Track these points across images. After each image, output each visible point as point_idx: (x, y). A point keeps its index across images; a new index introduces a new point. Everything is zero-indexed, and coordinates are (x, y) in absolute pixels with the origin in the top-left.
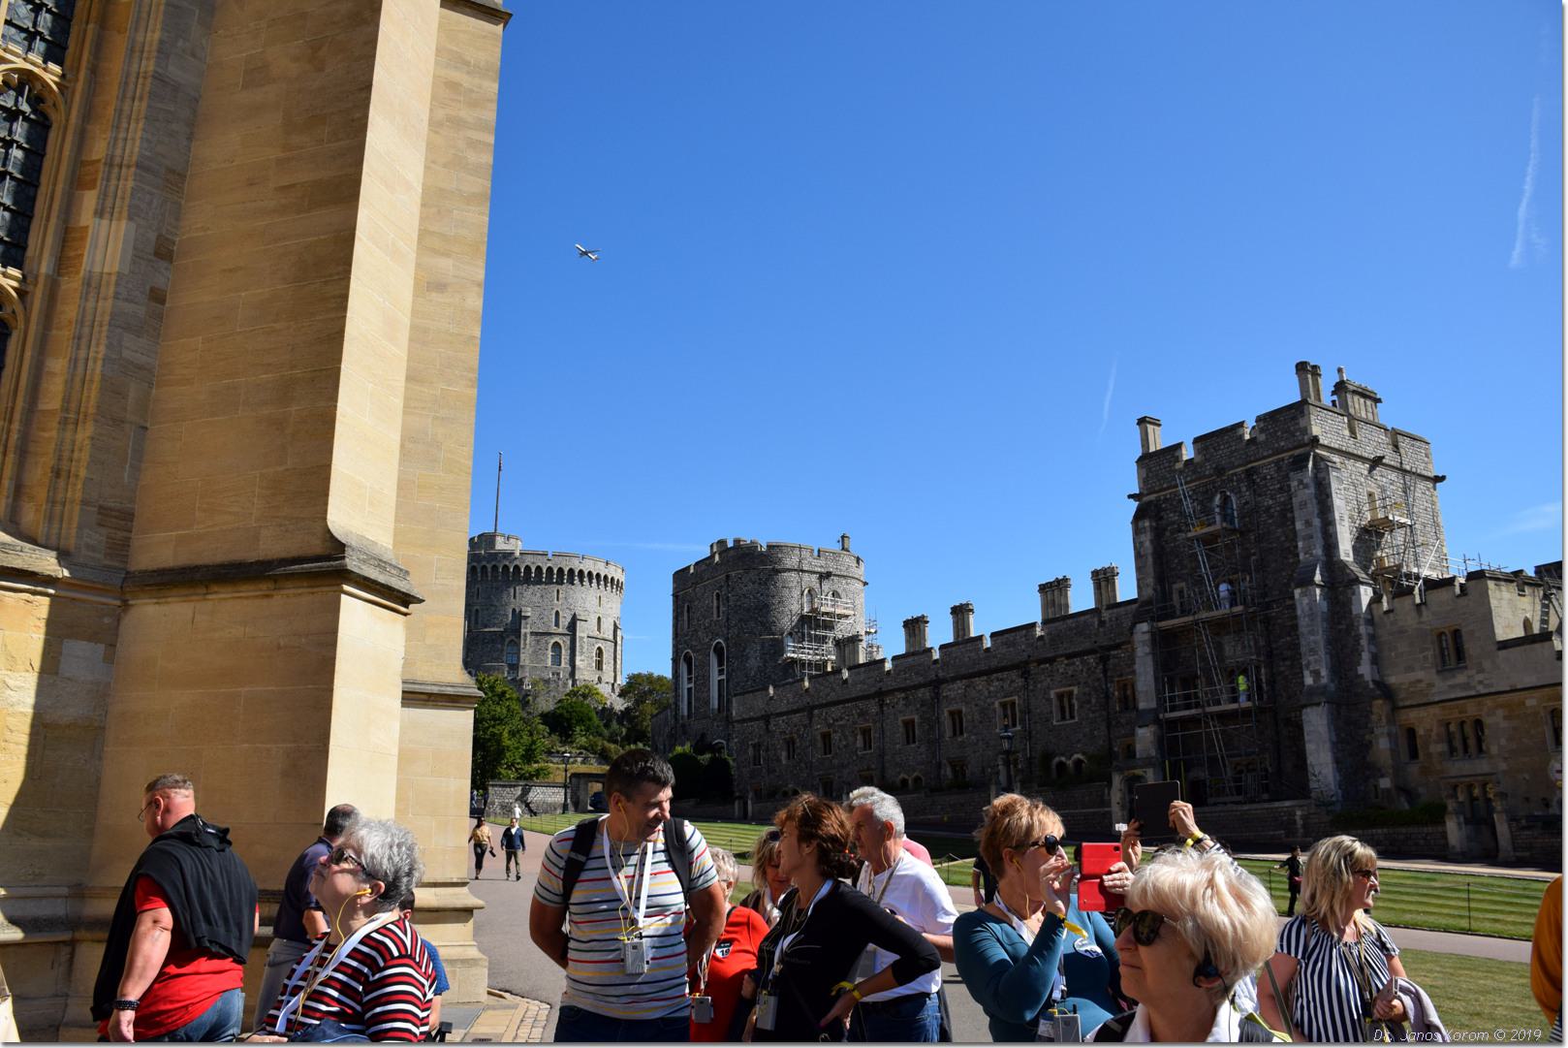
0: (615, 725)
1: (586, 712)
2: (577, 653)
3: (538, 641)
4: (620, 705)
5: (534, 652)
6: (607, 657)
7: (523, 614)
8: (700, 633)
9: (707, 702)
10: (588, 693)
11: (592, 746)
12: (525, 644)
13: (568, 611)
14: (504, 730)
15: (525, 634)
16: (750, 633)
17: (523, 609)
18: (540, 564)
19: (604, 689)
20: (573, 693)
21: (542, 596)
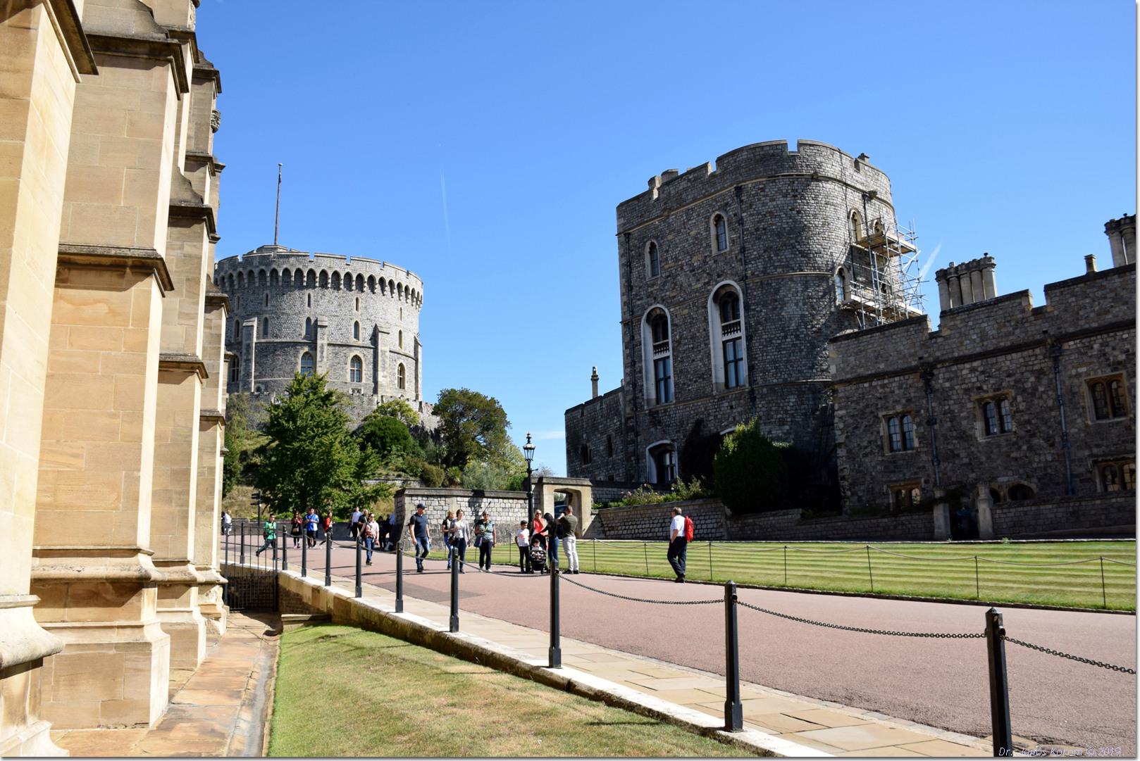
0: (431, 444)
1: (401, 428)
2: (380, 369)
4: (432, 422)
5: (332, 366)
6: (409, 374)
7: (319, 323)
8: (681, 279)
9: (706, 374)
10: (393, 410)
11: (409, 465)
12: (322, 357)
13: (368, 322)
14: (335, 439)
17: (320, 318)
18: (338, 270)
19: (414, 406)
20: (382, 410)
21: (340, 305)
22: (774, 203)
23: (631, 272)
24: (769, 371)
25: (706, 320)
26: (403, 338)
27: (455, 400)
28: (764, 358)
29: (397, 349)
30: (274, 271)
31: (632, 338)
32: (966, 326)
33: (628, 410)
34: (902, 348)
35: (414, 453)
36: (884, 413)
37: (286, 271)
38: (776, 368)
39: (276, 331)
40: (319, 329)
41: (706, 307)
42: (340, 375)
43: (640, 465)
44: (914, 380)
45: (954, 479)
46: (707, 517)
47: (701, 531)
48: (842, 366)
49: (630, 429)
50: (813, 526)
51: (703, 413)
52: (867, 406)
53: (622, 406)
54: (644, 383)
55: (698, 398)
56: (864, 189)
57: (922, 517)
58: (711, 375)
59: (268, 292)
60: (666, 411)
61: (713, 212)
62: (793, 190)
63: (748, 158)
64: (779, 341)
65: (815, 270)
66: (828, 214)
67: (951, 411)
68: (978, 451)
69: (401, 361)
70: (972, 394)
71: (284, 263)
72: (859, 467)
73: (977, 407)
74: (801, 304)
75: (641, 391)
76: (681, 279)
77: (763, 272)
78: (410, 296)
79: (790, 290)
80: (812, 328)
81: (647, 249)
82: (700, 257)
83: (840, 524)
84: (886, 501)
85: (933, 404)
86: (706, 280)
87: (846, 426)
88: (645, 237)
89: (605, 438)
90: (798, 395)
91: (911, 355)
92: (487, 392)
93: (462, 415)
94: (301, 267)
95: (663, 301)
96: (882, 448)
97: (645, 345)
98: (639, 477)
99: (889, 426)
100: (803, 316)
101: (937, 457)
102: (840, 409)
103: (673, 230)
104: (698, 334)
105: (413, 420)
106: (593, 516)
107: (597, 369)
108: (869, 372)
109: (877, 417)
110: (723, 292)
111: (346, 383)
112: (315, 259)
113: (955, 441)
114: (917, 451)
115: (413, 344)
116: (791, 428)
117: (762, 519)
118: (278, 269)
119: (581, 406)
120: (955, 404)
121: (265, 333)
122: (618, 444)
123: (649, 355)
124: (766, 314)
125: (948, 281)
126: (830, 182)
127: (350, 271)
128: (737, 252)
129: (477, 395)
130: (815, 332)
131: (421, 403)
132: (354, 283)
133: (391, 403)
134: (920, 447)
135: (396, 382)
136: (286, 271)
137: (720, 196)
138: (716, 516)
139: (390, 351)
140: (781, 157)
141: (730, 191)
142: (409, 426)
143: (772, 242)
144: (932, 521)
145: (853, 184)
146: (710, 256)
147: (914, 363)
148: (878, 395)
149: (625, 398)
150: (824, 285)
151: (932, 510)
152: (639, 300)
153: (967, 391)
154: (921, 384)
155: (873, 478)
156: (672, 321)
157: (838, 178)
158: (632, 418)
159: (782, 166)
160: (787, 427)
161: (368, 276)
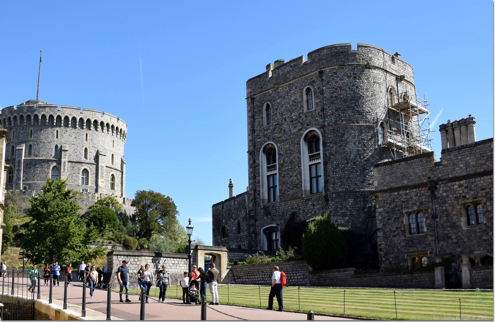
0: (130, 224)
2: (99, 177)
3: (73, 167)
4: (131, 211)
5: (70, 175)
7: (63, 149)
8: (285, 126)
9: (298, 185)
10: (107, 203)
11: (116, 237)
12: (64, 169)
13: (93, 148)
14: (71, 219)
15: (65, 162)
16: (345, 120)
17: (63, 145)
18: (75, 116)
19: (120, 201)
20: (100, 202)
21: (76, 138)
22: (342, 81)
23: (254, 122)
24: (337, 184)
25: (299, 152)
26: (114, 159)
27: (145, 197)
28: (334, 176)
29: (110, 165)
30: (36, 116)
31: (254, 162)
32: (457, 159)
33: (251, 205)
34: (418, 171)
35: (119, 229)
36: (406, 211)
37: (44, 116)
38: (341, 182)
39: (36, 153)
40: (63, 152)
41: (299, 144)
42: (75, 180)
43: (258, 239)
44: (425, 191)
45: (448, 252)
46: (297, 272)
47: (293, 280)
48: (381, 181)
49: (252, 217)
50: (362, 279)
51: (296, 209)
52: (396, 206)
53: (247, 203)
54: (261, 189)
55: (293, 199)
56: (397, 74)
57: (428, 274)
58: (301, 185)
59: (32, 128)
60: (273, 207)
61: (305, 86)
62: (354, 74)
63: (327, 54)
64: (343, 166)
65: (366, 123)
66: (374, 89)
67: (447, 210)
68: (463, 235)
69: (113, 173)
70: (460, 200)
71: (42, 111)
72: (391, 243)
73: (463, 209)
74: (357, 143)
75: (259, 194)
76: (285, 126)
77: (334, 123)
78: (119, 133)
79: (351, 135)
80: (363, 158)
81: (265, 108)
82: (297, 113)
83: (378, 277)
84: (406, 264)
85: (436, 206)
86: (300, 128)
87: (383, 218)
88: (263, 101)
89: (236, 222)
90: (354, 199)
91: (423, 176)
92: (165, 193)
93: (149, 206)
94: (52, 114)
95: (274, 139)
96: (404, 232)
97: (262, 166)
98: (257, 246)
99: (409, 219)
100: (358, 151)
101: (437, 238)
102: (380, 207)
103: (281, 97)
104: (294, 160)
105: (119, 209)
106: (228, 270)
107: (232, 180)
108: (398, 186)
109: (402, 213)
110: (310, 135)
111: (79, 185)
112: (61, 109)
113: (449, 229)
114: (426, 234)
115: (120, 162)
116: (349, 219)
117: (331, 274)
118: (39, 115)
119: (222, 203)
120: (449, 206)
121: (30, 154)
122: (244, 225)
123: (264, 172)
124: (336, 149)
125: (447, 131)
126: (377, 70)
127: (83, 117)
128: (319, 111)
129: (159, 195)
130: (365, 160)
131: (124, 198)
132: (85, 124)
133: (106, 199)
134: (427, 232)
135: (109, 185)
136: (44, 116)
137: (310, 76)
138: (303, 272)
139: (106, 167)
140: (347, 53)
141: (315, 74)
142: (117, 212)
143: (340, 105)
144: (433, 277)
145: (390, 71)
146: (302, 113)
147: (425, 181)
148: (403, 200)
149: (249, 198)
150: (372, 132)
151: (434, 270)
152: (259, 138)
153: (457, 198)
154: (429, 194)
155: (398, 250)
156: (279, 152)
157: (382, 67)
158: (253, 210)
159: (348, 59)
160: (347, 218)
161: (94, 120)
